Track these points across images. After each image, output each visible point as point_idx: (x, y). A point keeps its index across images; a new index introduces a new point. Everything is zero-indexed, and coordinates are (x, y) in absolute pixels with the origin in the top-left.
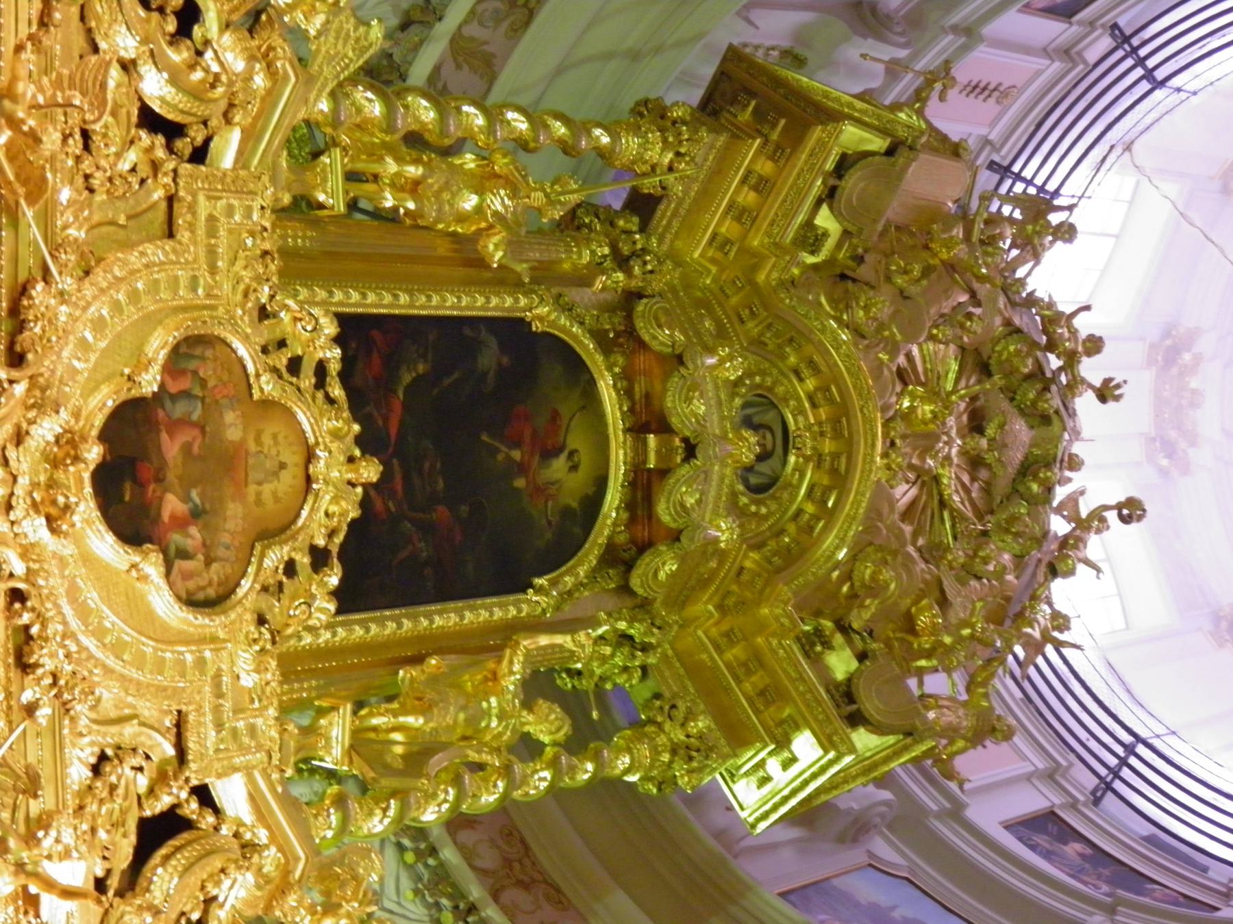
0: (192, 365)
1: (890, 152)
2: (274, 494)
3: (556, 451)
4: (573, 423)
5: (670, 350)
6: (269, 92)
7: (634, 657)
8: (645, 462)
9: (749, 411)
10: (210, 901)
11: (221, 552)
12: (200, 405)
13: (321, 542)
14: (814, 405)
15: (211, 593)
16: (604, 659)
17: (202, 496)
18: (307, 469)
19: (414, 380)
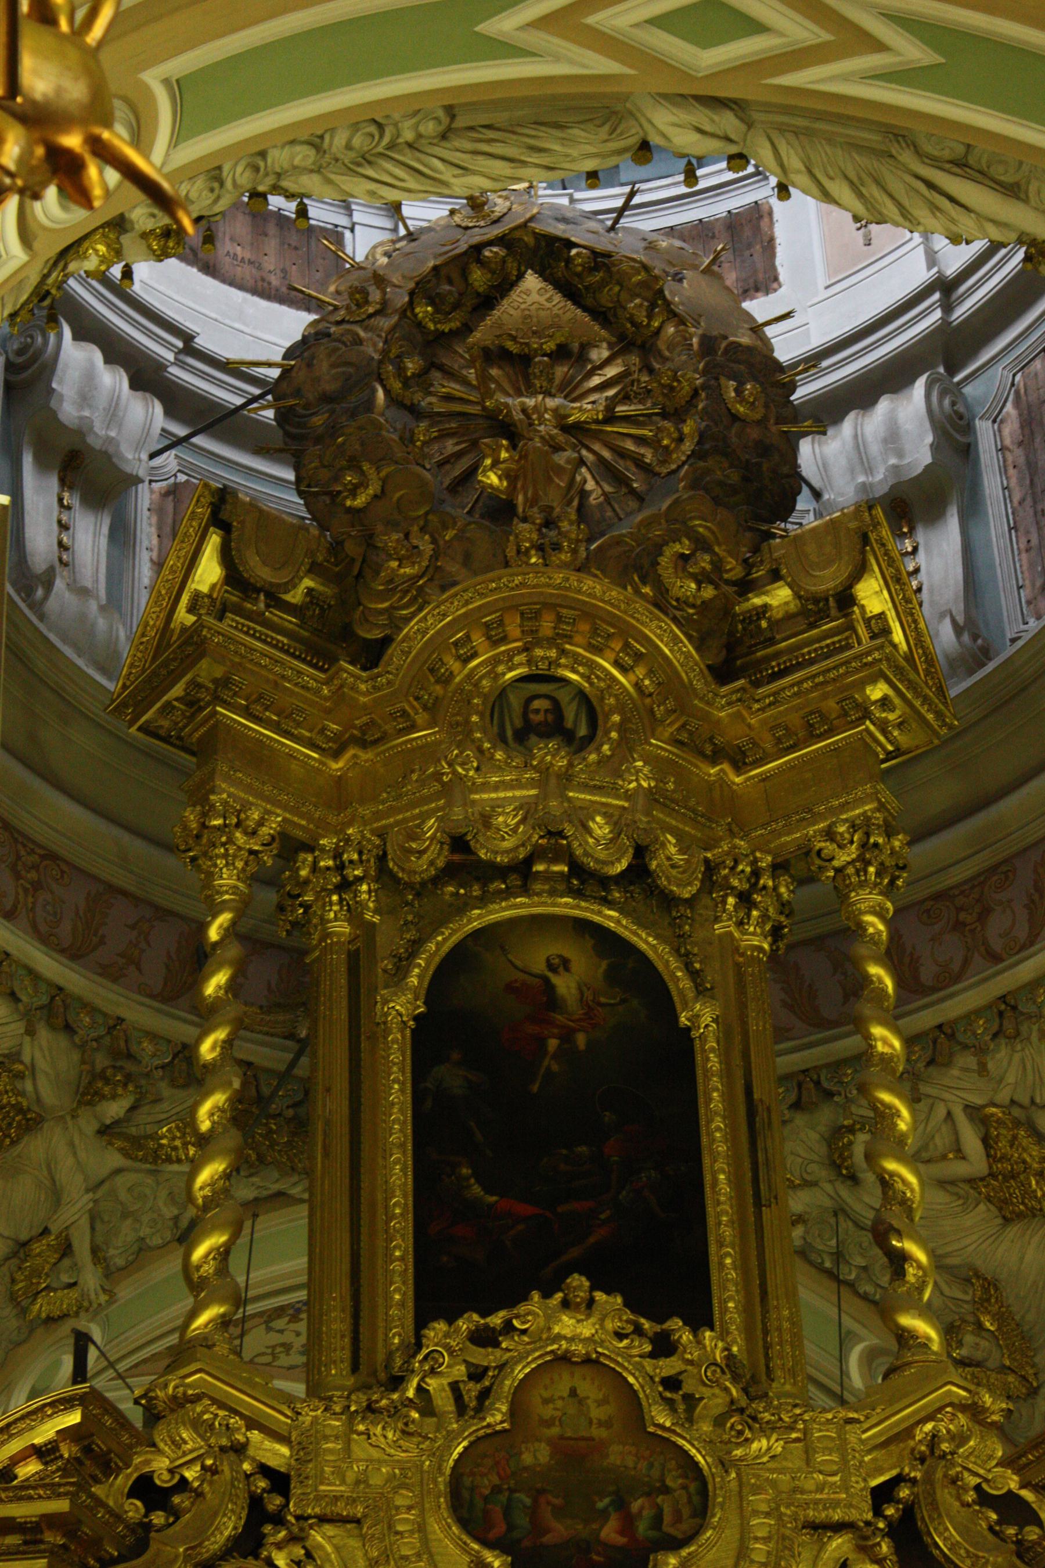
0: (479, 1503)
1: (225, 527)
2: (600, 1403)
3: (549, 987)
4: (518, 963)
5: (446, 847)
6: (214, 1401)
7: (764, 887)
8: (562, 873)
9: (509, 733)
10: (984, 1499)
11: (655, 1473)
12: (517, 1495)
13: (648, 1348)
14: (504, 639)
15: (693, 1487)
16: (765, 917)
17: (602, 1496)
18: (577, 1363)
19: (478, 1181)
